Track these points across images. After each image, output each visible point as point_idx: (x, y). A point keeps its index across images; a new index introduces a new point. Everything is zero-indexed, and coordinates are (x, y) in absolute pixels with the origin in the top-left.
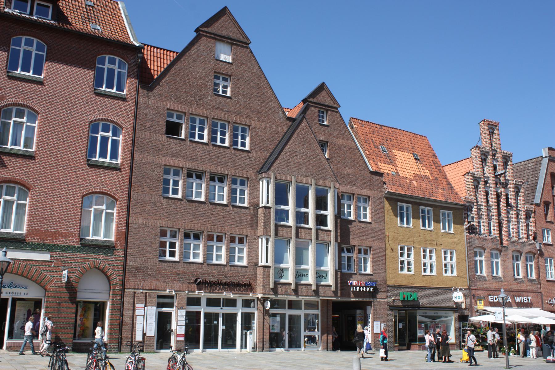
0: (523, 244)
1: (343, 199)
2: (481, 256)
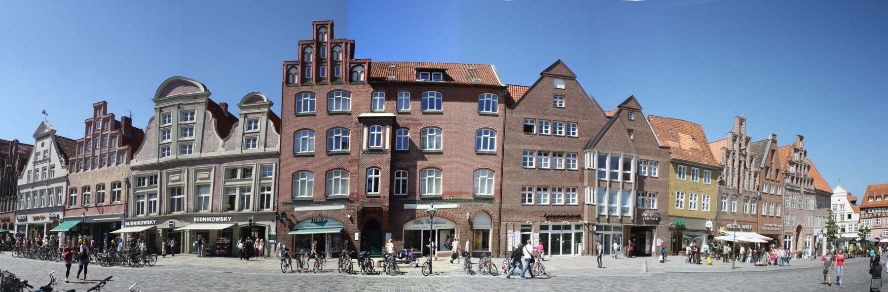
0: (751, 193)
1: (641, 164)
2: (725, 199)
